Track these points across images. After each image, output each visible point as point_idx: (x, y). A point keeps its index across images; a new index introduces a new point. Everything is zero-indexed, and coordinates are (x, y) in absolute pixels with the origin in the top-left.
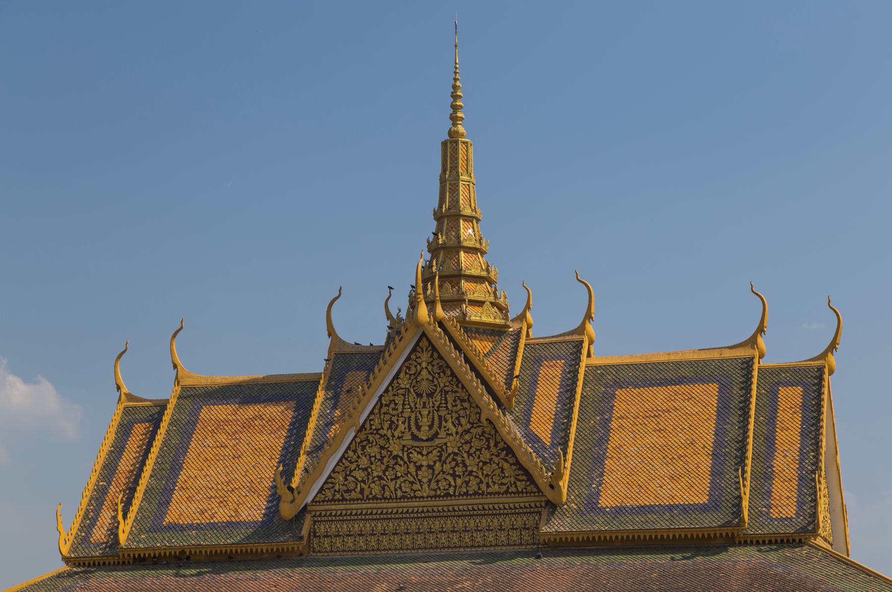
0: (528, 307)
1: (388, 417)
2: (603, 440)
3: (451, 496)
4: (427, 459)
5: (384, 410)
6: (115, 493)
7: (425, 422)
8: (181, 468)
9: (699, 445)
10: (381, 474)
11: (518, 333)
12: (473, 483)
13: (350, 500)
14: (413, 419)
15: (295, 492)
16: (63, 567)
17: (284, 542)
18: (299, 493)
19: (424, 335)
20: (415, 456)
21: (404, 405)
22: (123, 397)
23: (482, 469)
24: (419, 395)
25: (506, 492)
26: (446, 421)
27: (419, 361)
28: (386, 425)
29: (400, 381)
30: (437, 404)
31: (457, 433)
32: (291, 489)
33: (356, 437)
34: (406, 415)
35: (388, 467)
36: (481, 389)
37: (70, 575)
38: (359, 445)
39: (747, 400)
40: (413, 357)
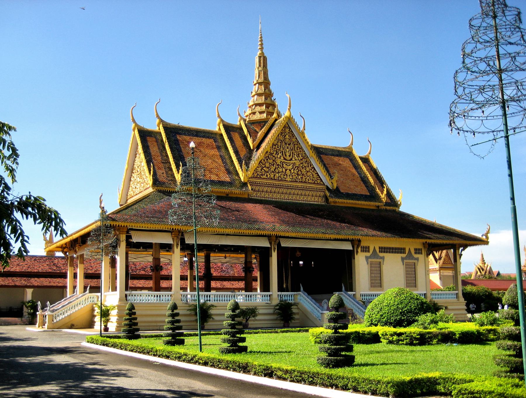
5: (274, 147)
7: (288, 154)
20: (284, 165)
21: (280, 146)
24: (286, 144)
26: (294, 155)
28: (275, 153)
30: (292, 148)
31: (298, 160)
35: (276, 168)
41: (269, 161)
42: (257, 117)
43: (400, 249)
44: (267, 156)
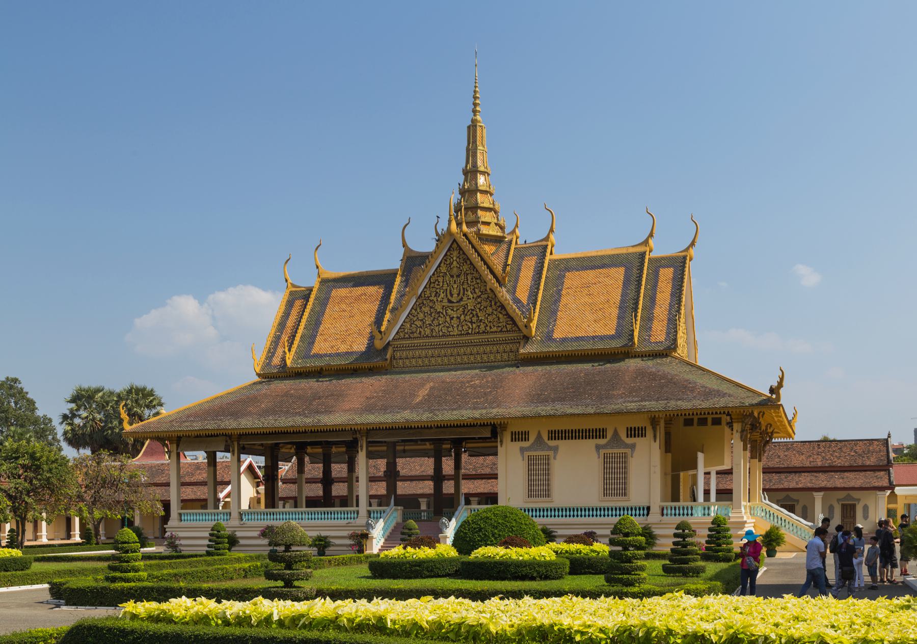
0: (517, 226)
1: (434, 289)
2: (557, 301)
3: (470, 334)
4: (456, 314)
5: (432, 285)
6: (285, 338)
7: (455, 292)
8: (321, 323)
9: (612, 302)
10: (430, 322)
11: (510, 242)
12: (482, 326)
13: (414, 338)
14: (448, 292)
15: (383, 334)
16: (257, 379)
17: (377, 362)
18: (385, 334)
19: (455, 241)
21: (443, 282)
22: (289, 285)
23: (487, 318)
24: (452, 276)
25: (501, 331)
26: (467, 291)
27: (452, 256)
28: (433, 294)
29: (441, 268)
30: (462, 281)
31: (473, 298)
32: (380, 332)
33: (416, 301)
34: (444, 288)
35: (434, 318)
36: (487, 272)
37: (260, 383)
38: (418, 306)
39: (641, 276)
40: (448, 254)
44: (421, 302)
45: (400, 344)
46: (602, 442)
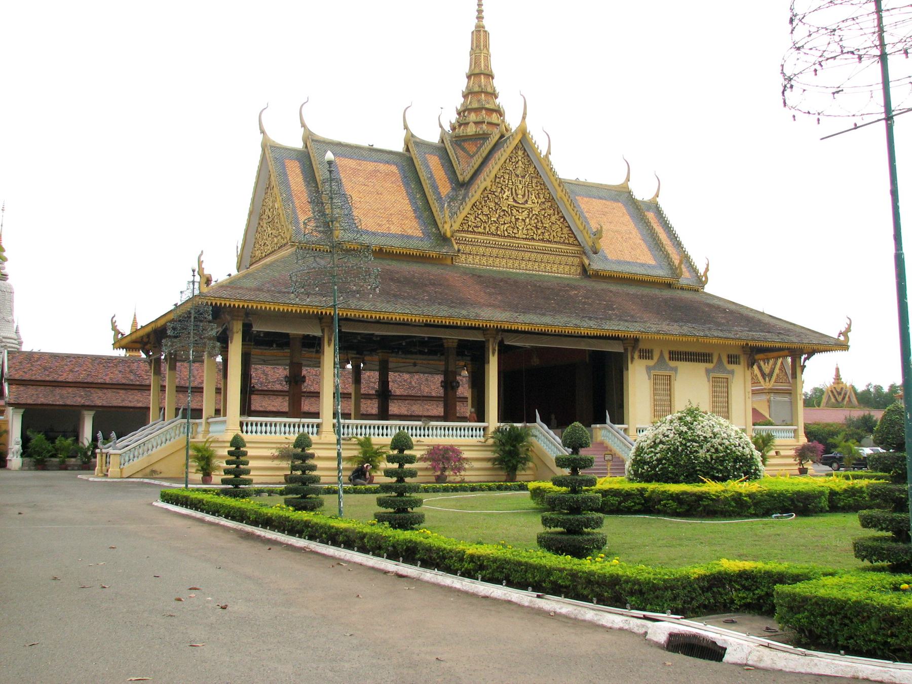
1: (500, 185)
5: (498, 180)
7: (519, 192)
10: (495, 219)
14: (514, 190)
20: (514, 211)
21: (509, 180)
26: (532, 194)
28: (499, 190)
31: (538, 203)
41: (489, 204)
42: (471, 130)
43: (704, 355)
44: (486, 195)
45: (463, 237)
46: (710, 366)
